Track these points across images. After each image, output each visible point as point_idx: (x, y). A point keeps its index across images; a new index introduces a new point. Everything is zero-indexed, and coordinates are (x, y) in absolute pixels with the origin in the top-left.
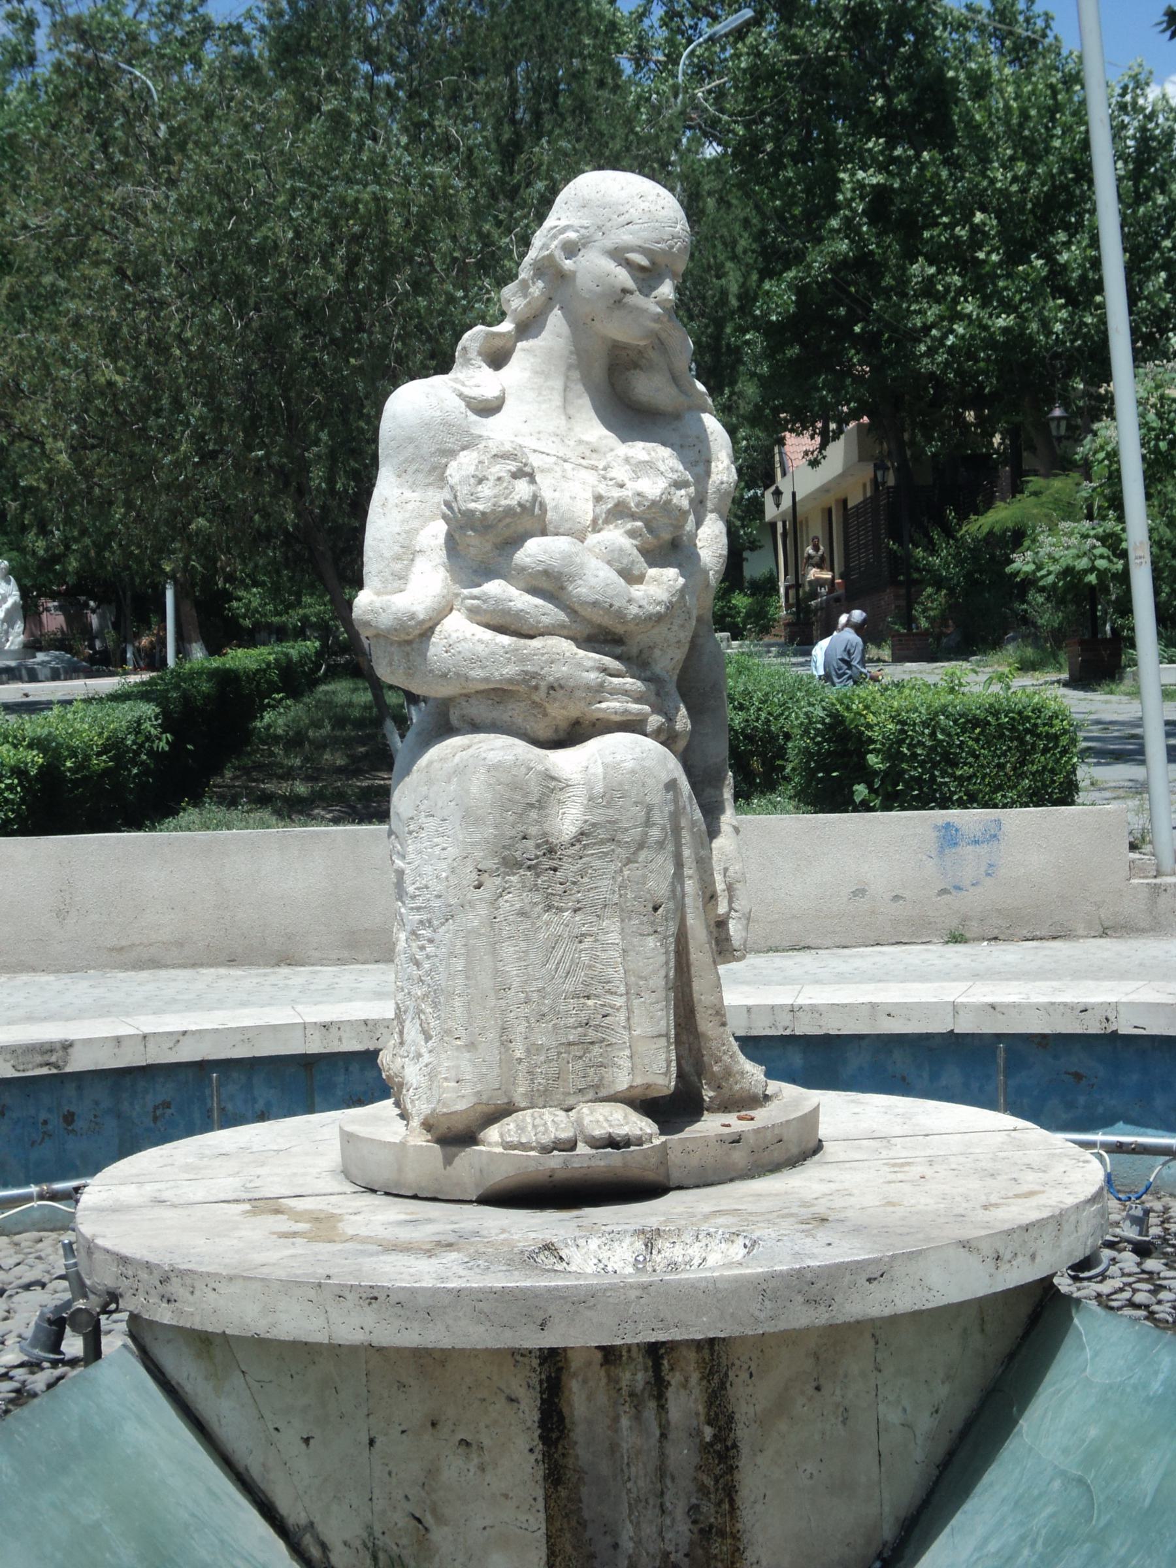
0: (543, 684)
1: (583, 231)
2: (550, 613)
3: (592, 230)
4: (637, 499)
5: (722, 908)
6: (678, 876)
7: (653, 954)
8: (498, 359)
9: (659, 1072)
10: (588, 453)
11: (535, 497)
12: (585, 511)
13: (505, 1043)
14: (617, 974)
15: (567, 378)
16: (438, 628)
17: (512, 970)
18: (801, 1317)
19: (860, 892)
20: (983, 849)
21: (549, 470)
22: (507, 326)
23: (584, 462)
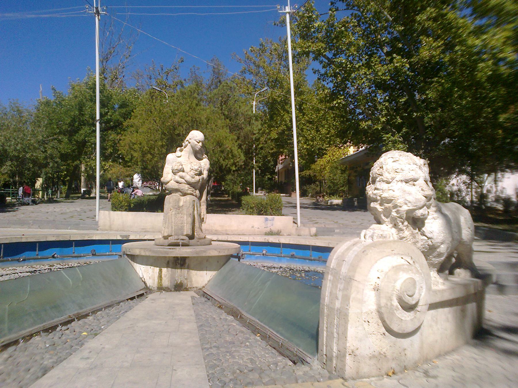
2: (183, 181)
5: (202, 217)
6: (194, 211)
7: (190, 220)
8: (181, 151)
9: (190, 232)
13: (172, 228)
14: (185, 222)
18: (195, 255)
19: (253, 227)
22: (183, 148)
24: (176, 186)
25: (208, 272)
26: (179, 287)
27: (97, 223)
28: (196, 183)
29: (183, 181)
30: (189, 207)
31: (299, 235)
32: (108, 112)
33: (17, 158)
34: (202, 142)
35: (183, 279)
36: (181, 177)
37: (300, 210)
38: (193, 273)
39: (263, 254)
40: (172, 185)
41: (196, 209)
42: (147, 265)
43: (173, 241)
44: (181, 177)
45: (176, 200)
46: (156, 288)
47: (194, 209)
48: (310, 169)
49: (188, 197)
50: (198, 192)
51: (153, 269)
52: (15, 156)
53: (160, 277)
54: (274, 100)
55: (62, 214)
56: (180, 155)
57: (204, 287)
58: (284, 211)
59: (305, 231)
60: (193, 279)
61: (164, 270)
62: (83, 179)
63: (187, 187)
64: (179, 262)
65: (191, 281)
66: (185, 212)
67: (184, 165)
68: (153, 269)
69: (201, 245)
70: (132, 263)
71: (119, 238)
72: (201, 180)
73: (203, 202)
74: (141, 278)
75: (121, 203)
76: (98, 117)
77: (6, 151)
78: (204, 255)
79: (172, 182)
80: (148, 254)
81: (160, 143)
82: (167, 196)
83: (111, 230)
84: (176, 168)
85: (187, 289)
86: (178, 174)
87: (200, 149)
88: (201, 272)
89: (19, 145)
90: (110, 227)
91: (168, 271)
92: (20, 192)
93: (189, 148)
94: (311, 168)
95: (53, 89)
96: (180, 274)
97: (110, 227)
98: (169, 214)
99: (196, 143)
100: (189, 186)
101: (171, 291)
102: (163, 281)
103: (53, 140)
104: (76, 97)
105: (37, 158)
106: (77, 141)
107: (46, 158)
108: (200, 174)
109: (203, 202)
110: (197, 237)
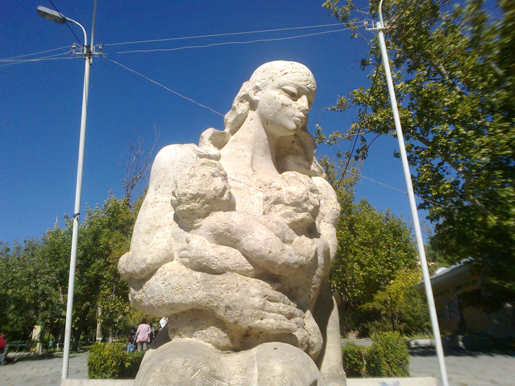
0: (223, 305)
1: (263, 81)
3: (267, 80)
4: (288, 195)
10: (263, 186)
11: (225, 189)
15: (254, 152)
16: (160, 270)
21: (240, 189)
23: (260, 189)
28: (302, 266)
34: (309, 93)
36: (226, 238)
37: (447, 364)
40: (171, 284)
44: (226, 238)
48: (373, 301)
62: (99, 325)
63: (256, 289)
72: (321, 260)
75: (105, 362)
79: (174, 268)
84: (192, 191)
87: (304, 127)
93: (252, 128)
94: (374, 299)
99: (284, 98)
100: (267, 288)
104: (91, 224)
106: (88, 278)
107: (35, 297)
108: (311, 231)
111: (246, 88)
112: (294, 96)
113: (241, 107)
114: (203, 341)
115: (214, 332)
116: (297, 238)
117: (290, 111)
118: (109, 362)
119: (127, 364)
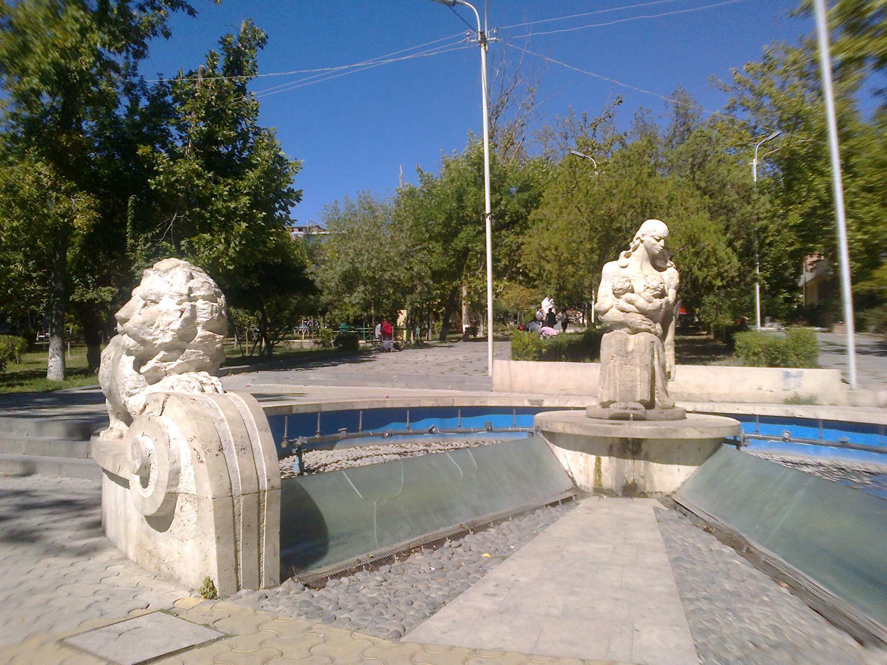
2: (632, 308)
5: (668, 370)
7: (646, 375)
8: (628, 256)
9: (647, 397)
12: (642, 289)
14: (639, 378)
17: (618, 376)
18: (658, 437)
19: (760, 389)
20: (797, 379)
22: (630, 251)
24: (620, 317)
25: (682, 467)
26: (631, 490)
27: (490, 380)
28: (655, 310)
29: (632, 308)
30: (644, 353)
31: (854, 406)
32: (501, 199)
33: (372, 279)
34: (665, 239)
35: (637, 477)
36: (630, 302)
38: (655, 466)
39: (784, 439)
40: (614, 315)
41: (656, 356)
42: (575, 450)
43: (619, 411)
44: (630, 302)
45: (620, 341)
46: (591, 490)
47: (653, 356)
48: (870, 279)
49: (642, 336)
50: (658, 327)
51: (586, 458)
52: (370, 278)
53: (598, 471)
54: (793, 153)
55: (437, 365)
56: (625, 265)
57: (674, 492)
58: (822, 359)
59: (866, 397)
60: (656, 478)
61: (605, 460)
63: (639, 318)
64: (630, 447)
65: (652, 482)
66: (637, 361)
67: (634, 281)
68: (586, 458)
69: (667, 419)
70: (551, 445)
71: (527, 404)
72: (664, 306)
73: (669, 344)
74: (567, 472)
76: (488, 210)
77: (356, 270)
78: (674, 436)
80: (577, 431)
81: (588, 246)
82: (605, 335)
83: (512, 391)
84: (619, 287)
85: (644, 495)
86: (624, 296)
87: (661, 252)
88: (669, 466)
89: (375, 261)
90: (511, 386)
91: (610, 462)
92: (378, 332)
93: (641, 251)
95: (419, 170)
96: (632, 468)
97: (511, 386)
98: (611, 365)
100: (643, 317)
101: (617, 496)
102: (603, 479)
103: (420, 250)
105: (399, 279)
106: (455, 250)
107: (412, 278)
108: (663, 294)
109: (669, 344)
110: (660, 404)
111: (638, 234)
112: (658, 241)
113: (637, 242)
114: (624, 331)
115: (627, 329)
116: (655, 300)
117: (656, 247)
118: (530, 346)
119: (544, 350)
